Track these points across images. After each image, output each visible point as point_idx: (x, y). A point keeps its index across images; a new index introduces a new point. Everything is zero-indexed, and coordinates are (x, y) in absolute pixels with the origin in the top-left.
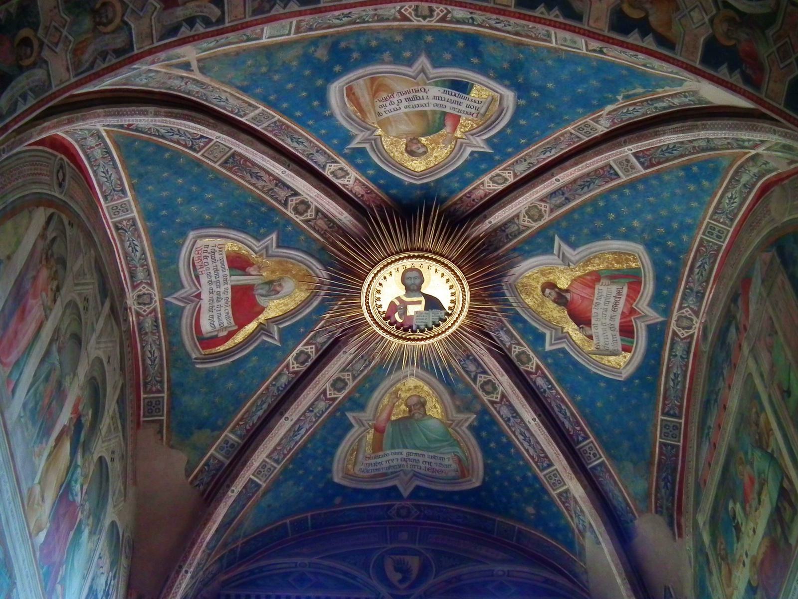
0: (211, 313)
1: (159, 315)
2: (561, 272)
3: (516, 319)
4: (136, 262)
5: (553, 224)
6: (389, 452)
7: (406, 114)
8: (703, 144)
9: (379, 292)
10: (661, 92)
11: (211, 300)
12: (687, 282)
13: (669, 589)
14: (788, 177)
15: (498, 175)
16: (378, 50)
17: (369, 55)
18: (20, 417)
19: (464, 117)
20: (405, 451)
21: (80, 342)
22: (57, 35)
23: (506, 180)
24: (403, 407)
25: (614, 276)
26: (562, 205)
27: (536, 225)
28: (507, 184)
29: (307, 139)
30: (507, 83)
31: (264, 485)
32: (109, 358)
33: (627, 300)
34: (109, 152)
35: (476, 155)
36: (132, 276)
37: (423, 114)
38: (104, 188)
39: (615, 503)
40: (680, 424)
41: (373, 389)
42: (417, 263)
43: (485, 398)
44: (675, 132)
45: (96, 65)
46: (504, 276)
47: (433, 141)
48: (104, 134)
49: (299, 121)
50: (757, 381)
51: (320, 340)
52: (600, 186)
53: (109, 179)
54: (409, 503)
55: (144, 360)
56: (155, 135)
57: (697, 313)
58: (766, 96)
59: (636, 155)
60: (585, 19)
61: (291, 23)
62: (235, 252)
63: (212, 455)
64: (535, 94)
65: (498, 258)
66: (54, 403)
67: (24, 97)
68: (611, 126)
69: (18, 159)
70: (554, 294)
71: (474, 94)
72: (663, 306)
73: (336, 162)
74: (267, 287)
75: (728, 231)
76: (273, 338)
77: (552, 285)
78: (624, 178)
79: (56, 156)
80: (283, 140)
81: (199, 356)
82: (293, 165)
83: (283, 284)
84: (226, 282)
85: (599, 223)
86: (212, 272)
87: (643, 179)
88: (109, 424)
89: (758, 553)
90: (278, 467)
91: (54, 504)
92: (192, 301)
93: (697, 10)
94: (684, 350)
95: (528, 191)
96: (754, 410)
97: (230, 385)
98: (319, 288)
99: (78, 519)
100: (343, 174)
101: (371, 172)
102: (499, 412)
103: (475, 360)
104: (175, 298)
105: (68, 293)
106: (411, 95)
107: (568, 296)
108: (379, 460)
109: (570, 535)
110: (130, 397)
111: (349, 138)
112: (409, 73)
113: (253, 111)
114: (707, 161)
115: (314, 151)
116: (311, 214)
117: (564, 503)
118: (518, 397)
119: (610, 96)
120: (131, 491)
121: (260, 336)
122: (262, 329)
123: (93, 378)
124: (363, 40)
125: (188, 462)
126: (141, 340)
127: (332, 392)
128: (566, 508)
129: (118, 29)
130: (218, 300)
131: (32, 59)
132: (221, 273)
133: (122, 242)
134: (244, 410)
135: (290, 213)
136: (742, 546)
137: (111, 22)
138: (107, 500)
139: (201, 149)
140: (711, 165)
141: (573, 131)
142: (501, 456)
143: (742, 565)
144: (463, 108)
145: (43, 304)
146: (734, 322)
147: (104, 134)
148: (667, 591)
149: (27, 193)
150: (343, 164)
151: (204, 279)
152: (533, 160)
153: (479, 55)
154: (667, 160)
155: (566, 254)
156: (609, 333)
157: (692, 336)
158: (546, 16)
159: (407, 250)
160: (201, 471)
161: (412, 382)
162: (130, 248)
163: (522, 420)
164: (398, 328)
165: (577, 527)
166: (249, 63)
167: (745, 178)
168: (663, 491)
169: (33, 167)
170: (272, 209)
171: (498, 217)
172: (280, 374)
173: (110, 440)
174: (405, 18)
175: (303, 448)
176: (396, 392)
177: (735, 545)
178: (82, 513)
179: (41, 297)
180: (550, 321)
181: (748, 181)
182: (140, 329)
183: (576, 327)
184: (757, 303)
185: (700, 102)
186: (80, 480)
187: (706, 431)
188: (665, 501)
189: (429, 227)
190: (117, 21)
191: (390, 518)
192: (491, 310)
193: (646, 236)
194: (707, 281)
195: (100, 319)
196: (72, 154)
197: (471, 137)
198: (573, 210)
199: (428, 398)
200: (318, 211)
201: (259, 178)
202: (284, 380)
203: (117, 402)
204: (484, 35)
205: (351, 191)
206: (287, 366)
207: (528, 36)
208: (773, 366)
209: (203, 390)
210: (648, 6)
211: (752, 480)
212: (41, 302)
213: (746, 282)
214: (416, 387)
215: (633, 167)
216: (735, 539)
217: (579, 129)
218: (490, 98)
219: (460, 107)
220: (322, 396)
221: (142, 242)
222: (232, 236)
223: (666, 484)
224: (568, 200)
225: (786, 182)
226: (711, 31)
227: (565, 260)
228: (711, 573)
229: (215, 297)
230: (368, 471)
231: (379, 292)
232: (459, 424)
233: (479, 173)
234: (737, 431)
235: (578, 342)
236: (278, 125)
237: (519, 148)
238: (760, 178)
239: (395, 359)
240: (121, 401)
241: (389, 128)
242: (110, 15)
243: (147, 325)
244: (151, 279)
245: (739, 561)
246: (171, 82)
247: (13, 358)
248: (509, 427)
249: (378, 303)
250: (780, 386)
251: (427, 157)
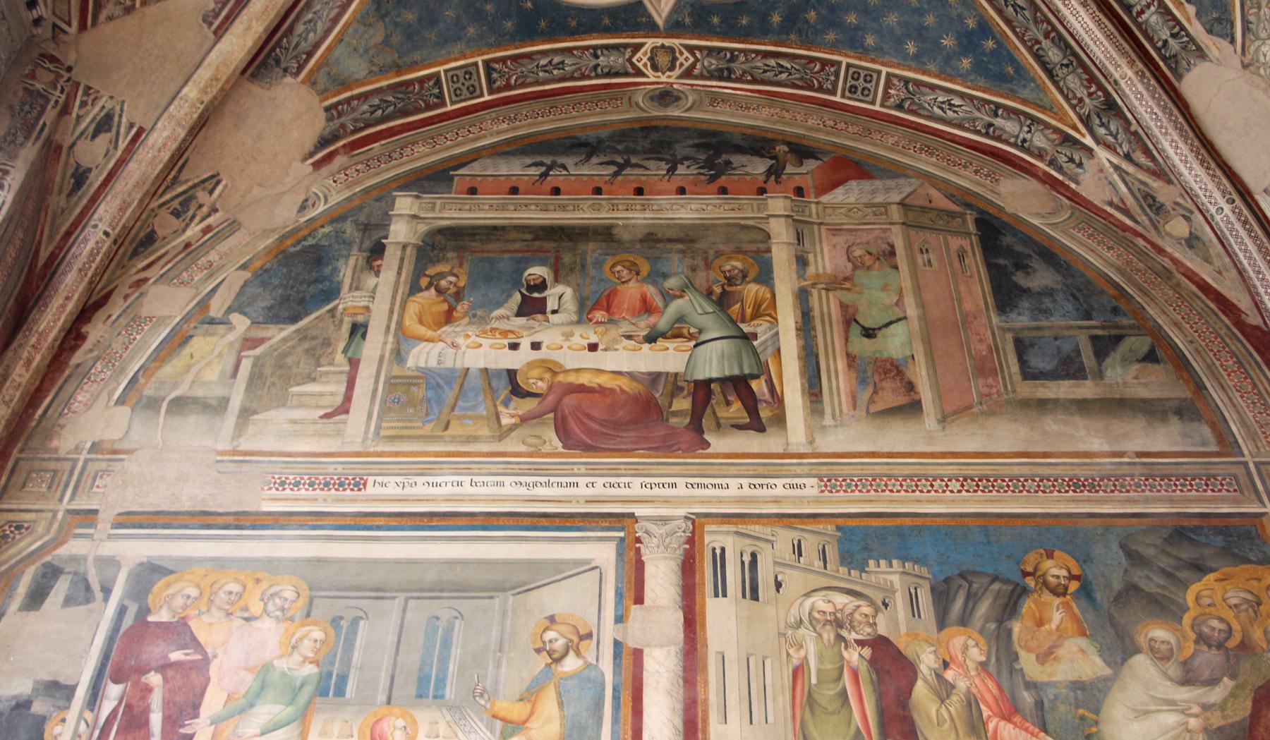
8: (1054, 55)
12: (741, 51)
13: (218, 182)
39: (300, 28)
40: (482, 95)
57: (688, 73)
72: (687, 20)
75: (873, 103)
89: (578, 370)
94: (611, 67)
114: (1013, 60)
140: (1010, 70)
143: (506, 342)
148: (214, 181)
157: (639, 73)
167: (1010, 126)
168: (366, 107)
181: (1001, 129)
184: (867, 205)
188: (352, 116)
194: (755, 81)
223: (378, 107)
245: (505, 334)
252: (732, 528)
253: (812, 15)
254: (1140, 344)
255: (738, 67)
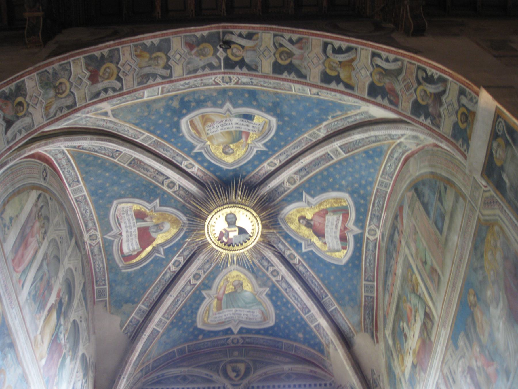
0: (128, 243)
1: (101, 245)
2: (308, 210)
3: (286, 236)
4: (88, 218)
5: (302, 186)
6: (225, 310)
7: (221, 133)
8: (374, 139)
9: (214, 226)
10: (350, 113)
11: (127, 236)
14: (417, 153)
15: (271, 162)
16: (205, 101)
17: (200, 103)
18: (27, 299)
19: (251, 132)
20: (234, 310)
21: (59, 260)
22: (37, 100)
23: (275, 164)
24: (231, 286)
25: (335, 211)
26: (305, 175)
27: (293, 187)
28: (277, 166)
29: (171, 149)
30: (272, 113)
31: (161, 331)
32: (76, 268)
33: (342, 223)
34: (69, 161)
35: (259, 152)
36: (86, 225)
37: (230, 133)
38: (68, 180)
39: (344, 328)
41: (214, 279)
42: (233, 210)
43: (274, 279)
44: (358, 133)
45: (57, 115)
46: (279, 214)
47: (236, 147)
48: (66, 152)
49: (167, 140)
50: (410, 259)
51: (186, 253)
52: (323, 164)
53: (71, 175)
54: (238, 336)
55: (95, 269)
56: (92, 151)
58: (401, 110)
59: (340, 147)
60: (308, 78)
61: (159, 89)
62: (138, 210)
63: (133, 317)
64: (287, 119)
65: (274, 205)
66: (46, 292)
67: (20, 132)
68: (326, 133)
69: (20, 165)
70: (305, 222)
71: (255, 120)
72: (361, 224)
73: (187, 160)
74: (156, 228)
76: (161, 254)
77: (303, 218)
78: (335, 160)
79: (42, 164)
80: (159, 150)
81: (123, 265)
82: (165, 163)
83: (164, 225)
84: (134, 226)
85: (325, 184)
86: (127, 221)
87: (346, 160)
88: (78, 303)
90: (168, 322)
91: (49, 345)
92: (118, 237)
93: (363, 69)
95: (287, 169)
96: (409, 274)
97: (140, 280)
98: (184, 226)
99: (63, 354)
100: (191, 166)
101: (206, 164)
102: (281, 286)
103: (267, 260)
104: (110, 236)
105: (51, 234)
106: (223, 123)
107: (312, 223)
108: (220, 315)
109: (322, 347)
110: (89, 289)
111: (193, 147)
112: (222, 112)
113: (142, 136)
114: (376, 148)
115: (175, 155)
116: (176, 188)
117: (318, 331)
118: (290, 277)
119: (324, 117)
120: (92, 337)
121: (154, 254)
122: (155, 250)
123: (67, 279)
124: (196, 96)
125: (121, 321)
126: (93, 259)
127: (194, 281)
128: (319, 333)
129: (68, 95)
130: (131, 235)
131: (23, 113)
132: (132, 222)
133: (80, 208)
134: (148, 293)
135: (165, 188)
136: (408, 344)
137: (64, 92)
138: (79, 342)
139: (117, 157)
141: (308, 137)
142: (283, 308)
144: (251, 128)
145: (37, 240)
146: (396, 230)
147: (66, 152)
149: (26, 183)
150: (191, 161)
151: (123, 225)
152: (289, 153)
153: (256, 100)
154: (356, 148)
155: (310, 201)
156: (335, 241)
157: (376, 239)
158: (288, 77)
159: (227, 204)
160: (128, 325)
161: (235, 273)
162: (84, 211)
163: (293, 289)
164: (225, 245)
165: (325, 342)
166: (138, 110)
167: (396, 155)
169: (29, 170)
170: (156, 186)
171: (273, 183)
172: (166, 273)
173: (78, 311)
174: (217, 84)
175: (180, 311)
176: (227, 279)
177: (405, 345)
178: (66, 349)
179: (36, 236)
180: (304, 237)
181: (397, 157)
182: (92, 253)
183: (317, 238)
185: (370, 117)
186: (63, 332)
187: (387, 287)
189: (238, 191)
190: (68, 92)
191: (228, 344)
192: (273, 232)
193: (349, 189)
195: (70, 248)
196: (51, 163)
197: (256, 143)
198: (311, 178)
199: (244, 281)
200: (180, 186)
201: (148, 171)
202: (168, 276)
203: (82, 291)
204: (258, 90)
205: (196, 175)
206: (169, 268)
207: (280, 89)
208: (417, 249)
209: (127, 283)
210: (339, 69)
211: (411, 310)
212: (36, 239)
213: (401, 208)
214: (237, 276)
215: (340, 153)
216: (404, 340)
217: (311, 135)
218: (264, 123)
219: (249, 128)
220: (188, 283)
221: (90, 207)
222: (136, 202)
223: (369, 317)
224: (308, 173)
225: (416, 155)
226: (371, 79)
227: (309, 204)
228: (394, 360)
229: (129, 234)
230: (215, 321)
231: (214, 226)
232: (261, 293)
233: (262, 162)
234: (402, 286)
235: (319, 246)
236: (156, 143)
237: (281, 147)
238: (403, 155)
239: (225, 261)
240: (84, 291)
241: (214, 141)
242: (64, 89)
243: (95, 251)
244: (96, 226)
246: (98, 123)
247: (21, 269)
248: (287, 293)
249: (214, 232)
250: (421, 260)
251: (234, 155)
252: (444, 365)
253: (362, 192)
254: (442, 188)
255: (377, 214)
